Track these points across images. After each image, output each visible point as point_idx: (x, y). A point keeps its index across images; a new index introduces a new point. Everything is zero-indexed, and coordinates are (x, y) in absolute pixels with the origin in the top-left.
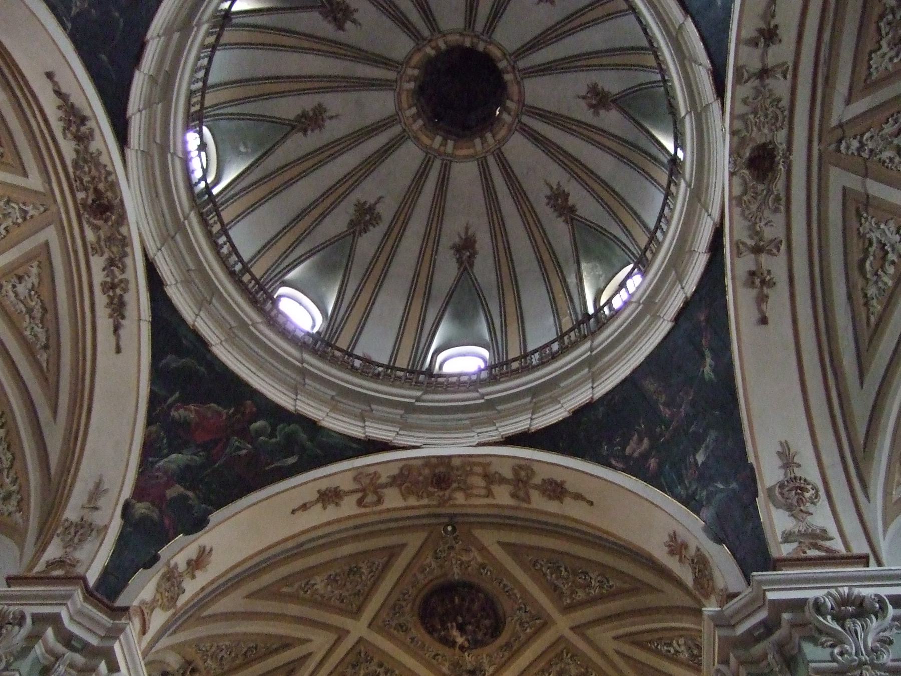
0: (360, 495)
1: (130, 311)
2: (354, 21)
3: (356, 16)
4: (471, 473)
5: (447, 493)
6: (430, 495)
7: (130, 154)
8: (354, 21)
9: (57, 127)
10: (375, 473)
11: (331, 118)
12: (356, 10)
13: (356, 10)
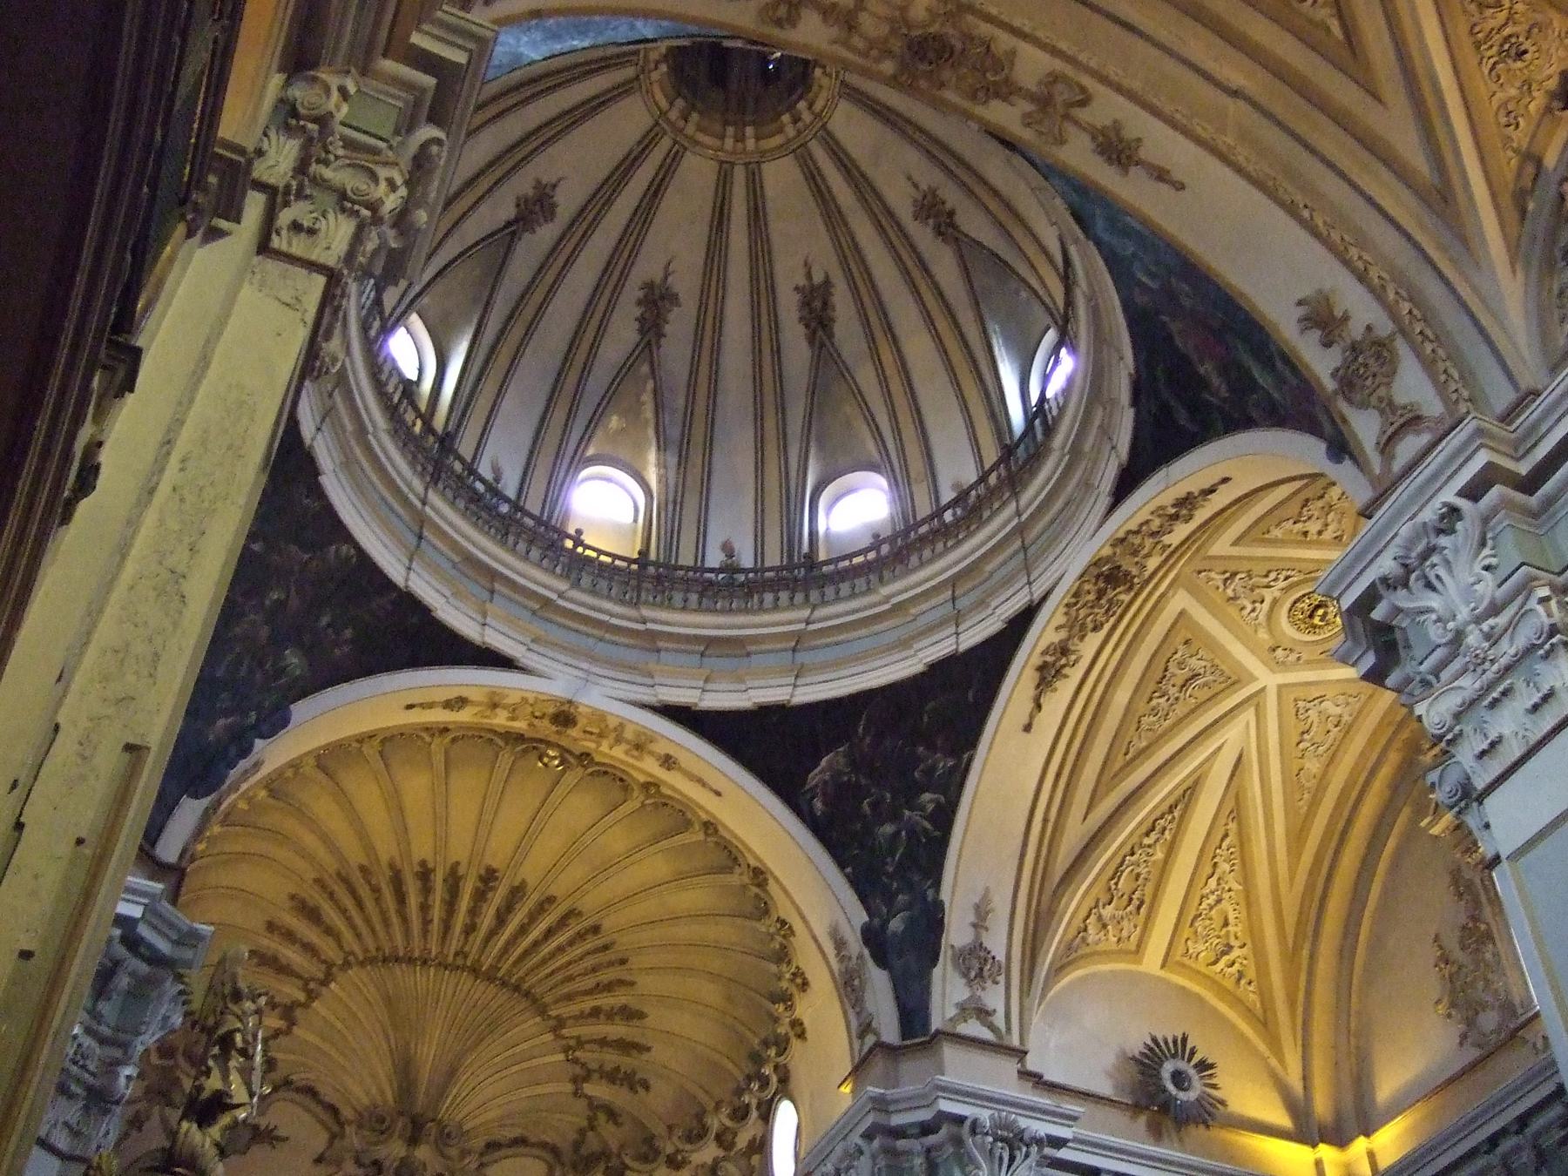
0: (1078, 113)
1: (1180, 491)
2: (809, 276)
3: (802, 282)
4: (872, 43)
5: (934, 29)
6: (968, 37)
7: (1038, 591)
8: (809, 276)
9: (1076, 674)
10: (1028, 125)
11: (916, 186)
12: (797, 288)
13: (797, 288)
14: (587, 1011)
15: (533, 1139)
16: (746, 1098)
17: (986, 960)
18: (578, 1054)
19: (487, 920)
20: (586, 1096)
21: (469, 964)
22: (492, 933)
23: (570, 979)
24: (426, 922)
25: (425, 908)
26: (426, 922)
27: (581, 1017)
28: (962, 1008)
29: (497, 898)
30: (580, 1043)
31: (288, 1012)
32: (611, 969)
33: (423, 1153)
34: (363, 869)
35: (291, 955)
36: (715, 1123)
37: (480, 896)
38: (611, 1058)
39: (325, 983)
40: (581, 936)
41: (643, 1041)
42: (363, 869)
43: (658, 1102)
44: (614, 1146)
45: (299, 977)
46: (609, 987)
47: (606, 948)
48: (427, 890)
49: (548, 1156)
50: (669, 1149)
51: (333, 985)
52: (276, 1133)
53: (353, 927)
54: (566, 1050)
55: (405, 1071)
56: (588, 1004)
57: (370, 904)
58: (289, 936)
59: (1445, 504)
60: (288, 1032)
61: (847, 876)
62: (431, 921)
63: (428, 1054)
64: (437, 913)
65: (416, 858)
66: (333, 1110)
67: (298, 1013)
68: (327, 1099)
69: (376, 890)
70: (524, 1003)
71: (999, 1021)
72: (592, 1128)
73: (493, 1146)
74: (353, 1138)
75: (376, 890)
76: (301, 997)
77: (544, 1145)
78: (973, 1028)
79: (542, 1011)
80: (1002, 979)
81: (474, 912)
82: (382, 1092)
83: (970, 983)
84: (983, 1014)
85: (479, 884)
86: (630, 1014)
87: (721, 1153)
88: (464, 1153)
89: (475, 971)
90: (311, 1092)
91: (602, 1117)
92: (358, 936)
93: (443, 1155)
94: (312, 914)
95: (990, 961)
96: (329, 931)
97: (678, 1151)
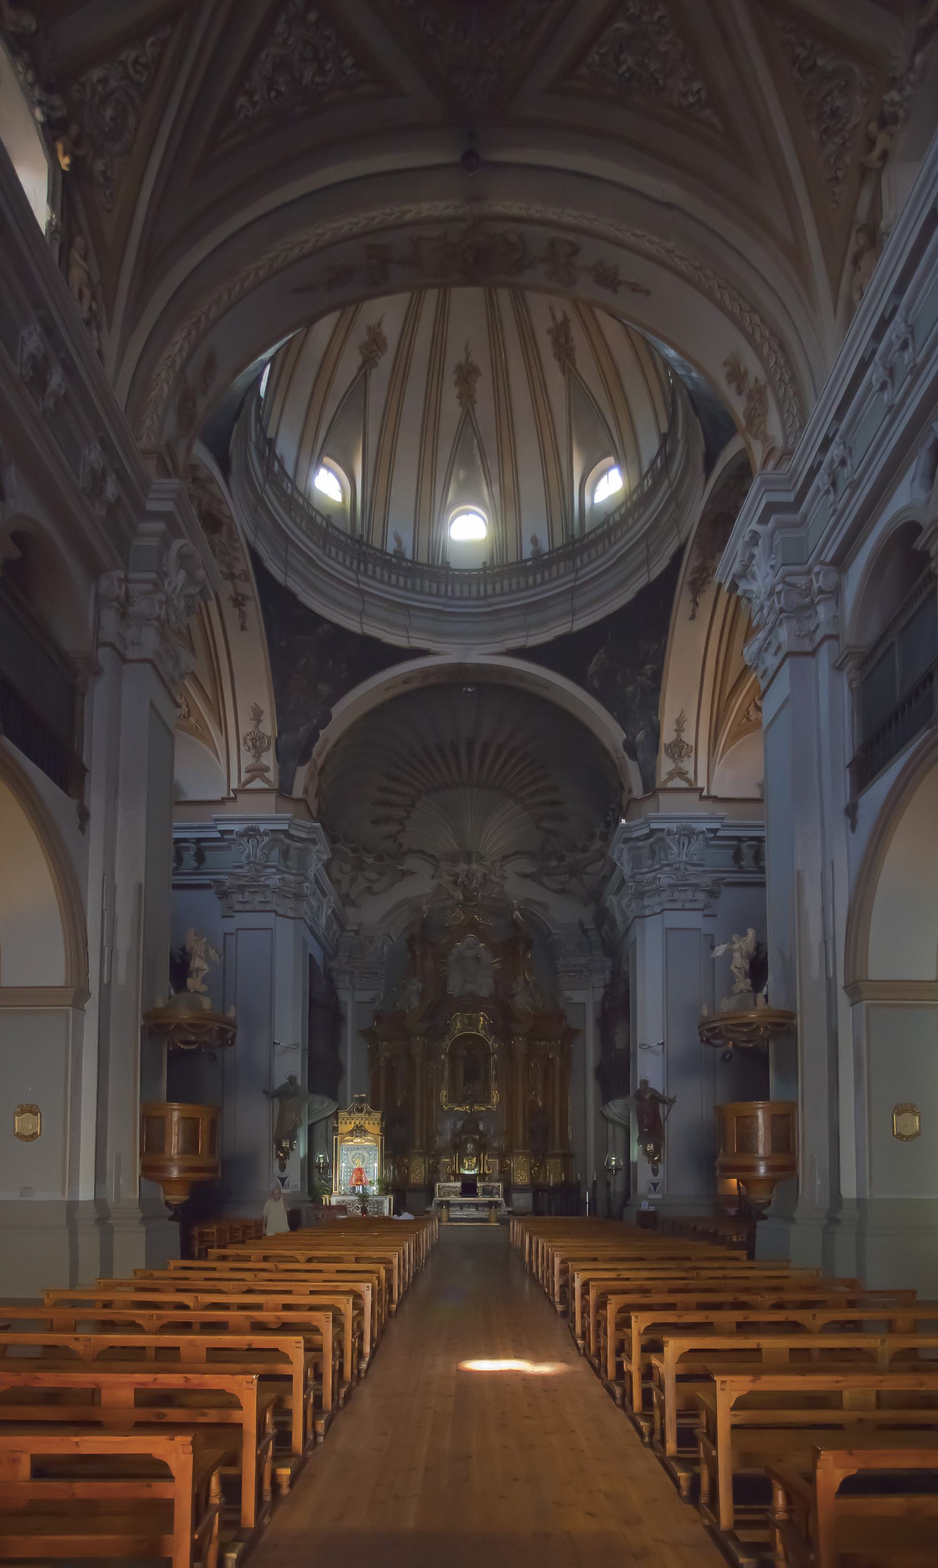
17: (683, 748)
28: (671, 775)
33: (474, 866)
59: (751, 531)
61: (614, 717)
66: (432, 856)
71: (691, 775)
73: (504, 857)
76: (404, 814)
78: (678, 783)
80: (693, 754)
83: (675, 760)
84: (682, 774)
90: (422, 852)
95: (686, 746)
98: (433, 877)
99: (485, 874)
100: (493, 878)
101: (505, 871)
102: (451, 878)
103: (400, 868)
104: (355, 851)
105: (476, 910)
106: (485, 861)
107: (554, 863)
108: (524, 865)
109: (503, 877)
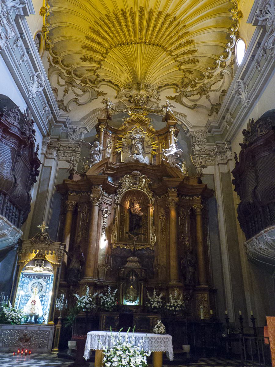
14: (178, 46)
15: (170, 84)
16: (227, 50)
18: (178, 59)
19: (145, 26)
20: (182, 70)
21: (143, 41)
22: (147, 30)
23: (171, 38)
24: (129, 30)
25: (127, 26)
26: (129, 30)
27: (177, 48)
29: (146, 17)
30: (178, 56)
31: (99, 62)
32: (182, 30)
33: (142, 92)
34: (106, 15)
35: (95, 46)
36: (218, 62)
37: (141, 17)
38: (187, 57)
39: (107, 54)
40: (171, 23)
41: (195, 49)
42: (106, 15)
43: (201, 65)
44: (192, 79)
45: (100, 53)
46: (182, 37)
47: (179, 23)
48: (126, 19)
49: (175, 87)
50: (207, 74)
51: (109, 54)
52: (104, 92)
53: (110, 36)
54: (174, 59)
55: (133, 73)
56: (177, 44)
57: (112, 28)
58: (93, 41)
60: (100, 67)
62: (130, 30)
63: (139, 68)
64: (131, 27)
65: (120, 9)
66: (117, 85)
67: (102, 63)
68: (115, 83)
69: (113, 22)
70: (160, 49)
72: (186, 77)
73: (160, 87)
74: (123, 91)
75: (113, 22)
76: (102, 58)
77: (174, 84)
79: (165, 50)
81: (141, 24)
82: (129, 80)
85: (139, 14)
86: (189, 42)
87: (222, 69)
88: (152, 91)
89: (145, 43)
90: (110, 82)
91: (187, 73)
92: (112, 39)
93: (148, 91)
94: (98, 33)
96: (103, 38)
97: (210, 73)
98: (116, 98)
99: (148, 97)
100: (152, 99)
101: (160, 95)
102: (127, 99)
103: (96, 89)
104: (69, 73)
105: (142, 111)
106: (149, 88)
107: (189, 89)
108: (172, 93)
109: (158, 99)
